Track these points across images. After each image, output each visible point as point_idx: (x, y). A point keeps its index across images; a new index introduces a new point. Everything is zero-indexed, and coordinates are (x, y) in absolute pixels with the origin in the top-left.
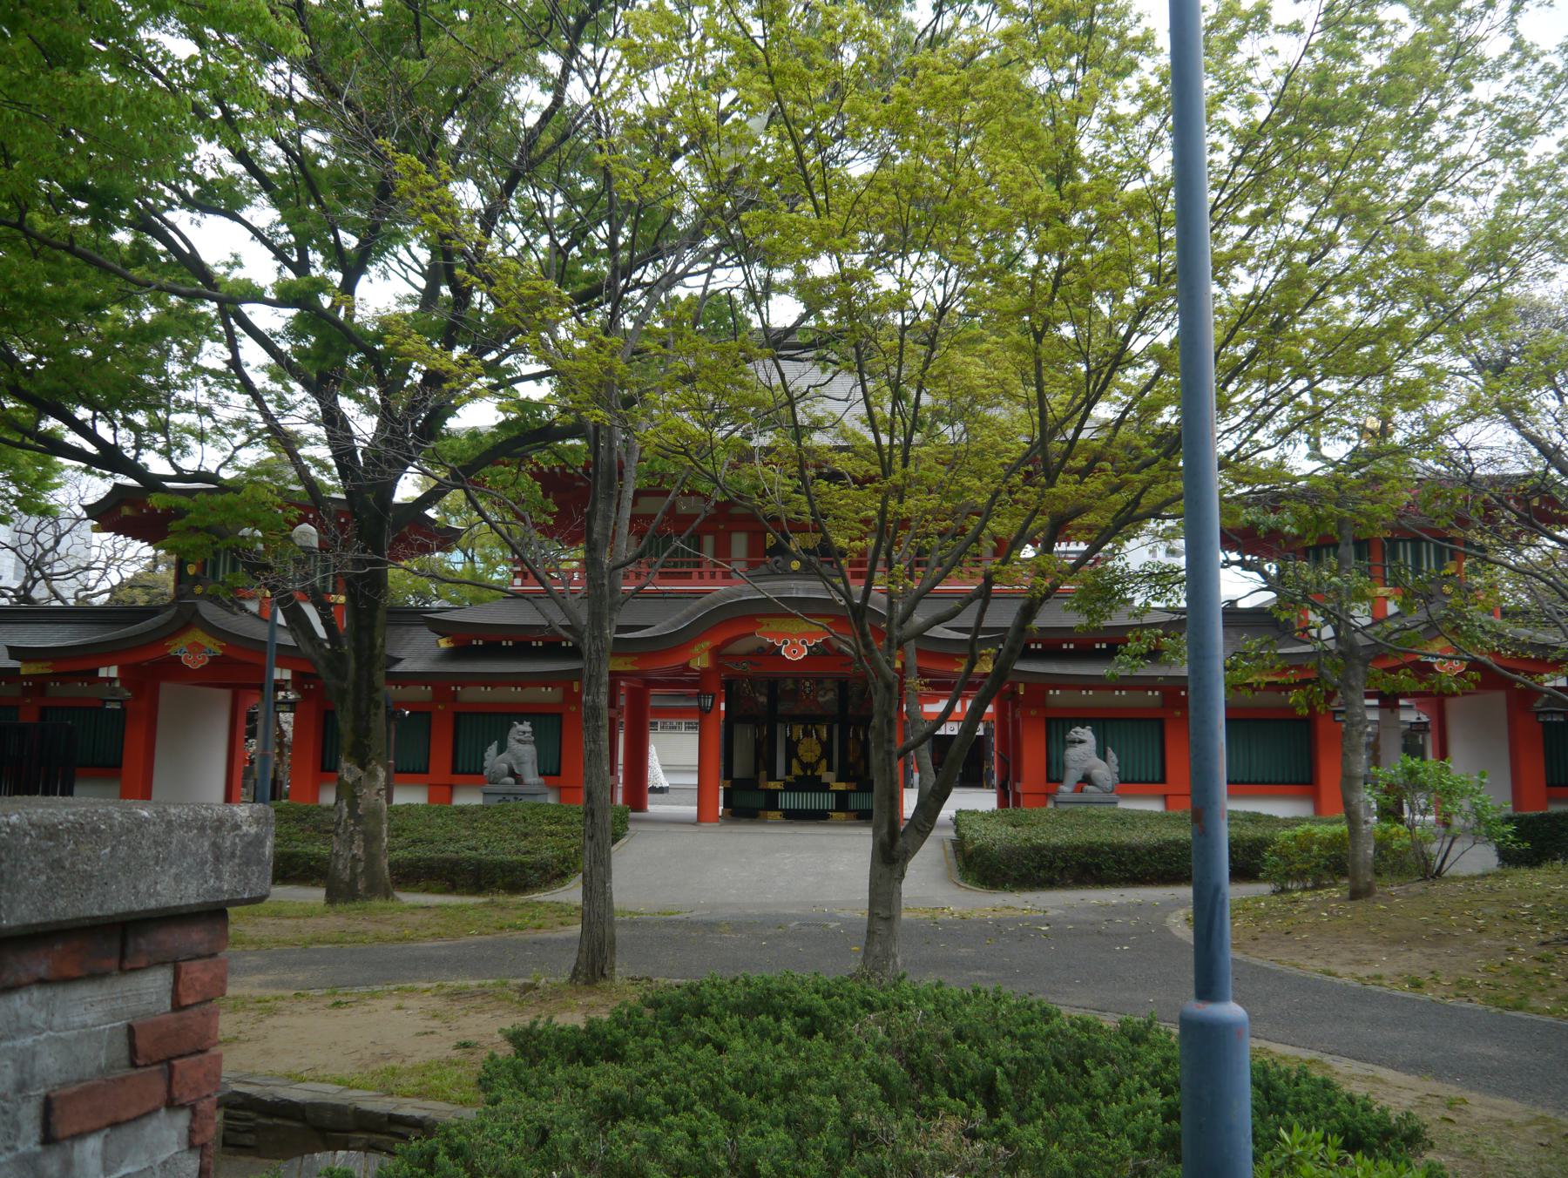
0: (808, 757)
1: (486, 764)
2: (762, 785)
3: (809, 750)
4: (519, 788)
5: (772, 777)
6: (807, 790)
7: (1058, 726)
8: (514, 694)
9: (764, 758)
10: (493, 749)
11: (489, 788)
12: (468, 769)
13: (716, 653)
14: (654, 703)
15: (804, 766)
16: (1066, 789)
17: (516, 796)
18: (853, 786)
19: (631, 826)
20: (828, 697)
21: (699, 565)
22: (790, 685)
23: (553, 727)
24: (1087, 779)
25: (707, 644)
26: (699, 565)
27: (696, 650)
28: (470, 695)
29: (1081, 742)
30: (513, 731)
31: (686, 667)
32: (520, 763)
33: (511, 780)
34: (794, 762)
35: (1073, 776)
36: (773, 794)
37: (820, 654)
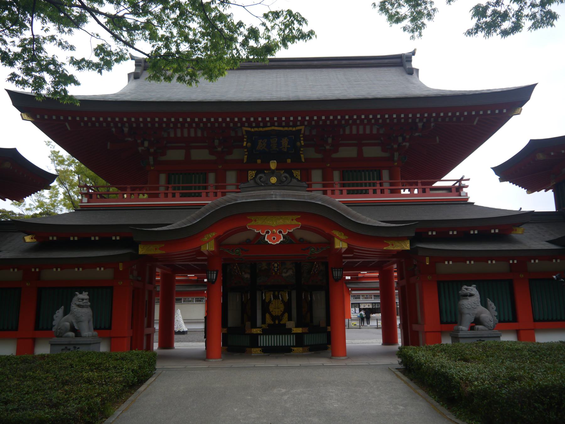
1: (54, 323)
2: (247, 332)
3: (277, 308)
4: (78, 339)
5: (254, 326)
6: (277, 334)
7: (450, 288)
8: (78, 273)
10: (60, 311)
11: (55, 340)
12: (43, 327)
13: (219, 241)
15: (274, 318)
16: (464, 328)
17: (75, 346)
18: (306, 330)
19: (158, 365)
21: (206, 188)
23: (100, 294)
24: (477, 321)
26: (206, 188)
27: (206, 239)
28: (53, 274)
29: (471, 295)
30: (75, 299)
31: (199, 253)
32: (79, 322)
33: (71, 334)
34: (267, 316)
35: (468, 319)
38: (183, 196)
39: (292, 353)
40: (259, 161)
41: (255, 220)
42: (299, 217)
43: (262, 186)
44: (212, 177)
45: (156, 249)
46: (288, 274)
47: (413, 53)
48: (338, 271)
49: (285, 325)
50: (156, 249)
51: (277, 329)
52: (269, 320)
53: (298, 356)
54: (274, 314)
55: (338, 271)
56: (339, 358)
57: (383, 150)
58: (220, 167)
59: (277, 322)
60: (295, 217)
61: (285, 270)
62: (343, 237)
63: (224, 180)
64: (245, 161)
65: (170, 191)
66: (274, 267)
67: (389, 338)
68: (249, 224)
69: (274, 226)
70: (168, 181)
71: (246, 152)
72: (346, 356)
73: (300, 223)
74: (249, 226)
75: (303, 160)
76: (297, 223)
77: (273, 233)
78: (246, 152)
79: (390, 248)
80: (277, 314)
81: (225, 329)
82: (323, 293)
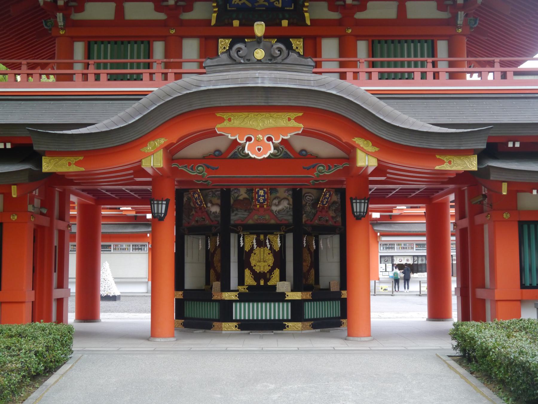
2: (215, 297)
3: (262, 260)
5: (226, 288)
9: (216, 268)
14: (104, 213)
15: (257, 276)
19: (77, 346)
20: (282, 206)
21: (149, 66)
22: (243, 194)
25: (162, 141)
26: (149, 66)
27: (149, 148)
31: (140, 171)
34: (247, 272)
37: (286, 152)
38: (113, 78)
39: (285, 331)
40: (236, 23)
41: (230, 120)
42: (301, 114)
43: (241, 63)
44: (159, 48)
45: (70, 164)
46: (280, 207)
48: (360, 203)
49: (274, 287)
50: (70, 164)
51: (263, 293)
52: (249, 280)
53: (294, 335)
54: (257, 269)
55: (360, 203)
56: (359, 339)
57: (441, 7)
58: (173, 32)
59: (262, 283)
61: (276, 201)
62: (370, 148)
63: (179, 55)
64: (213, 22)
65: (92, 70)
66: (259, 196)
67: (438, 311)
68: (219, 126)
69: (259, 128)
70: (89, 55)
71: (214, 7)
72: (370, 336)
73: (301, 125)
74: (219, 129)
75: (308, 22)
76: (296, 124)
77: (257, 140)
78: (214, 7)
79: (445, 167)
80: (262, 270)
81: (181, 293)
82: (336, 239)
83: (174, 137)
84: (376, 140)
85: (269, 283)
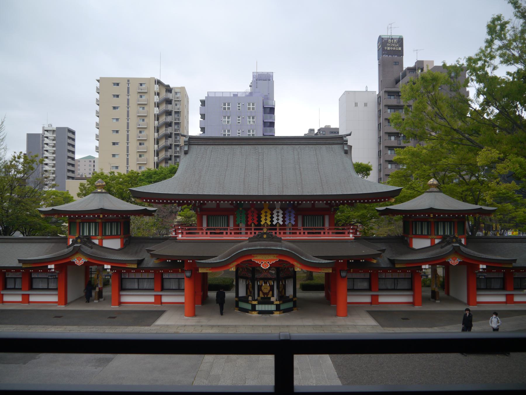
0: (266, 291)
2: (250, 302)
13: (238, 267)
15: (264, 294)
18: (281, 302)
34: (261, 292)
36: (254, 307)
47: (350, 135)
49: (270, 298)
51: (266, 301)
60: (275, 255)
62: (299, 265)
83: (239, 262)
84: (301, 264)
85: (269, 296)
